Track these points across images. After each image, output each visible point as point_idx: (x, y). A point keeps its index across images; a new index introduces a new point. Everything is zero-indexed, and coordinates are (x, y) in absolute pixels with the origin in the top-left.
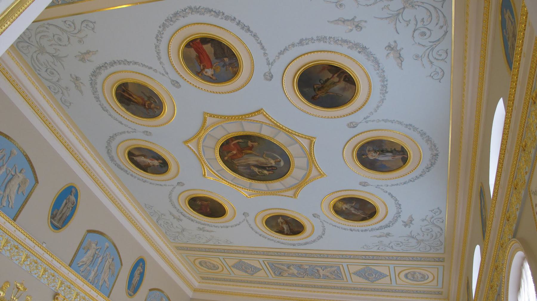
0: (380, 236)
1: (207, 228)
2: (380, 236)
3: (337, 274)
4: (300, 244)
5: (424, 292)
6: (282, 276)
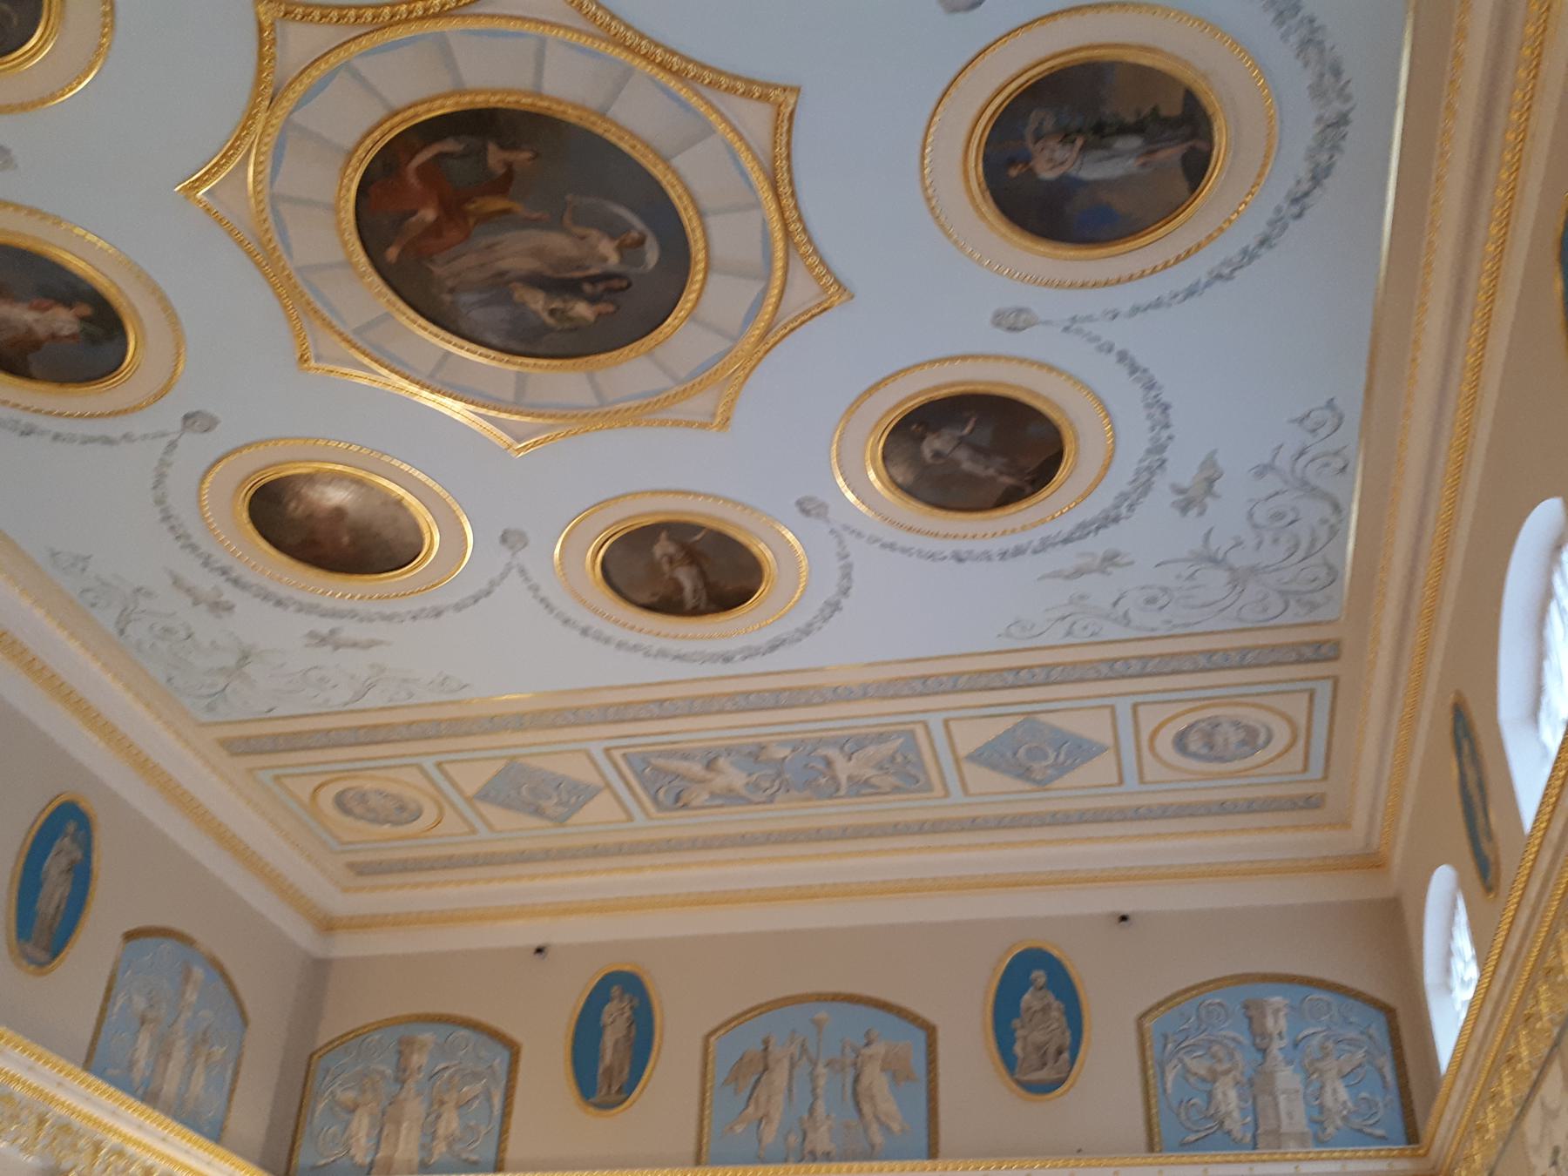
0: (1079, 572)
1: (350, 630)
2: (1079, 572)
3: (906, 772)
4: (750, 653)
5: (1251, 807)
6: (685, 806)
